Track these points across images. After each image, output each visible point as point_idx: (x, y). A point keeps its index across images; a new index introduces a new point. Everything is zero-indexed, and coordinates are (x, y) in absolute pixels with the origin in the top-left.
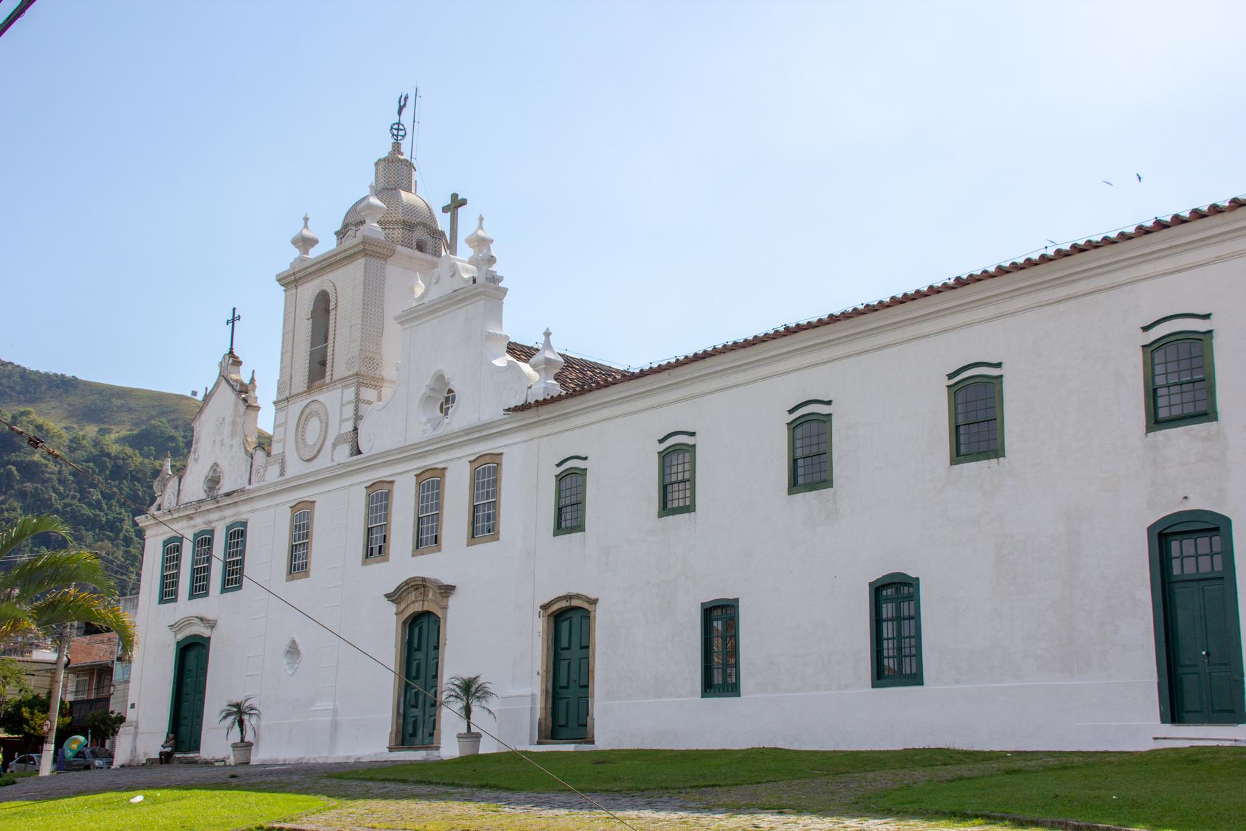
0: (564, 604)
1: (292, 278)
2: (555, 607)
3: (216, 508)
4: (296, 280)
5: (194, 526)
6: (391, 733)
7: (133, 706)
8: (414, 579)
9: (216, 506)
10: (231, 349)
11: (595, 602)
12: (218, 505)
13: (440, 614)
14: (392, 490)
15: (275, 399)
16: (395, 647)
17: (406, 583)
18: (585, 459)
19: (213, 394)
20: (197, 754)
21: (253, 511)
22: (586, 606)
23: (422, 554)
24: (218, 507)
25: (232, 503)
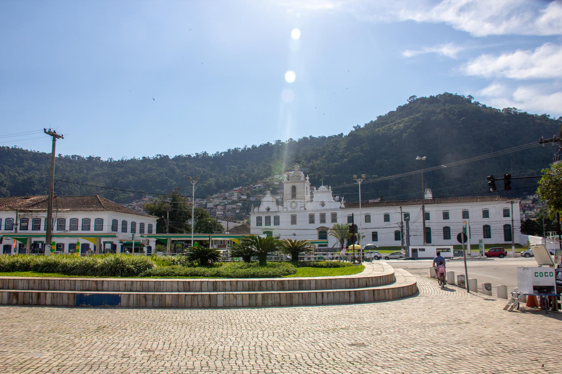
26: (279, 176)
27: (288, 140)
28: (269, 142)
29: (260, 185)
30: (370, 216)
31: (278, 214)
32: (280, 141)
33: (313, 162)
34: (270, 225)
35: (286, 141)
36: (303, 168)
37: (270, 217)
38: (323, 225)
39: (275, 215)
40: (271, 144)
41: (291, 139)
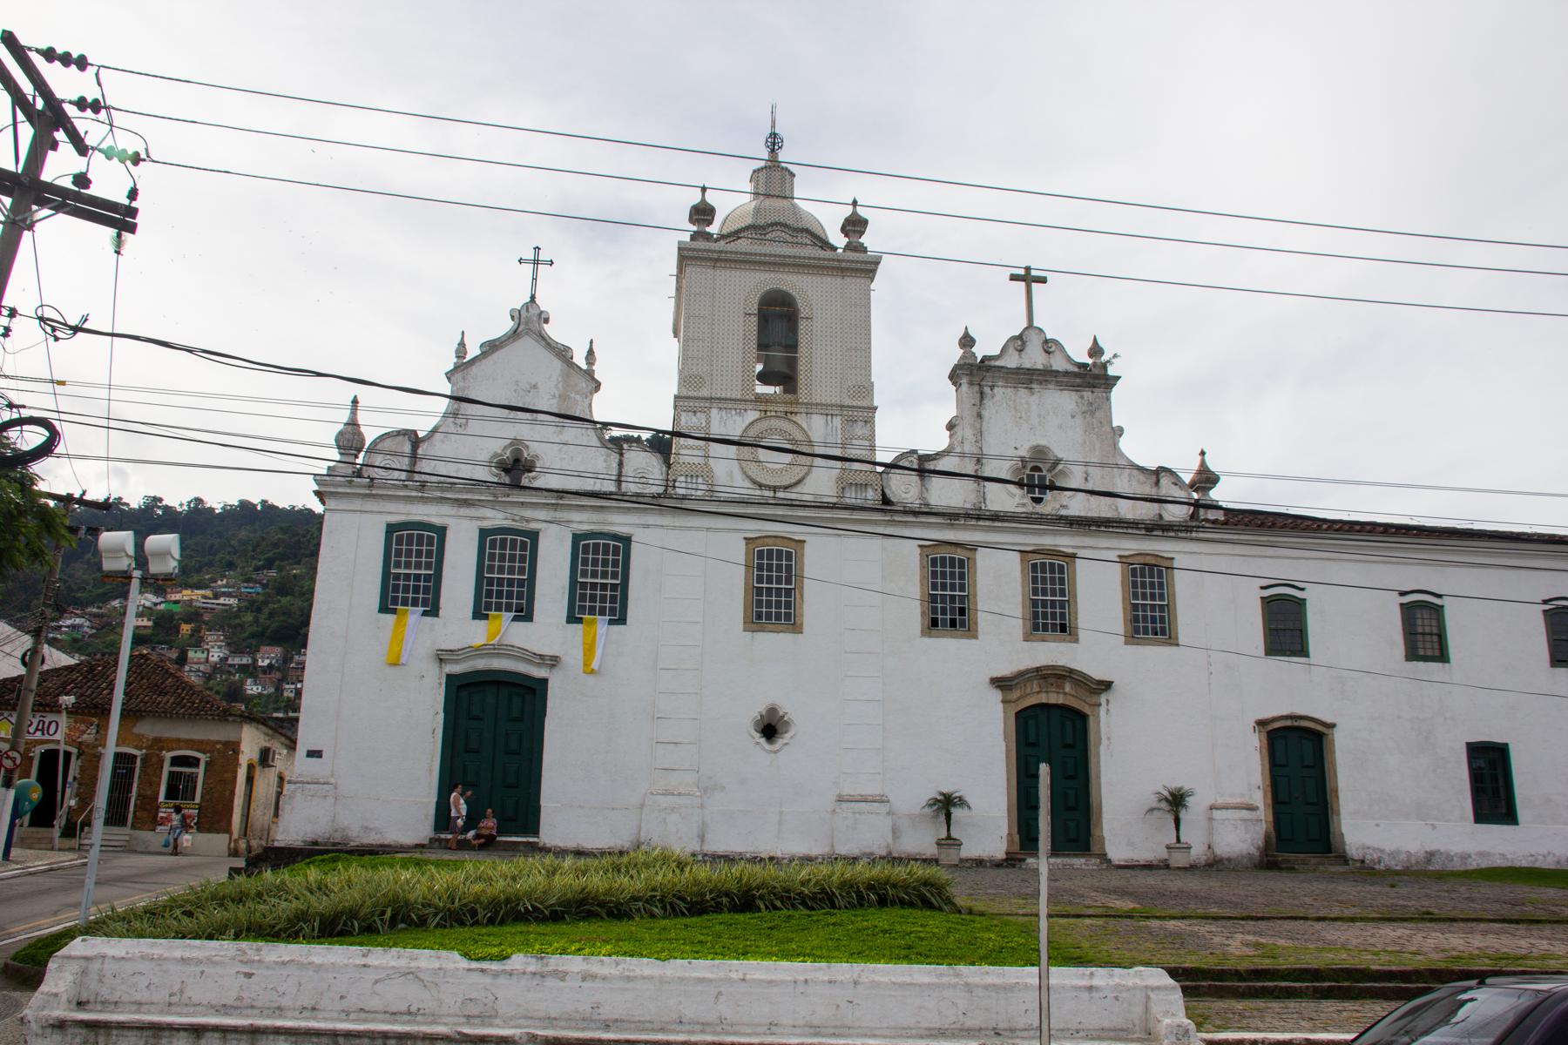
0: (1288, 723)
1: (715, 255)
2: (1277, 725)
3: (553, 504)
4: (717, 260)
5: (478, 518)
6: (1009, 834)
7: (314, 754)
8: (1054, 667)
9: (553, 502)
10: (533, 298)
11: (1332, 726)
12: (561, 502)
13: (1086, 710)
14: (975, 560)
15: (676, 393)
16: (1005, 738)
17: (1038, 669)
18: (1303, 589)
19: (502, 347)
20: (535, 840)
21: (647, 526)
22: (1320, 728)
23: (1043, 641)
24: (558, 504)
25: (591, 506)
26: (154, 599)
27: (190, 502)
28: (120, 498)
29: (78, 621)
30: (1438, 611)
31: (620, 522)
32: (161, 500)
33: (280, 569)
34: (525, 613)
35: (181, 505)
36: (246, 584)
37: (534, 536)
38: (1050, 653)
39: (585, 521)
40: (127, 505)
41: (199, 501)
